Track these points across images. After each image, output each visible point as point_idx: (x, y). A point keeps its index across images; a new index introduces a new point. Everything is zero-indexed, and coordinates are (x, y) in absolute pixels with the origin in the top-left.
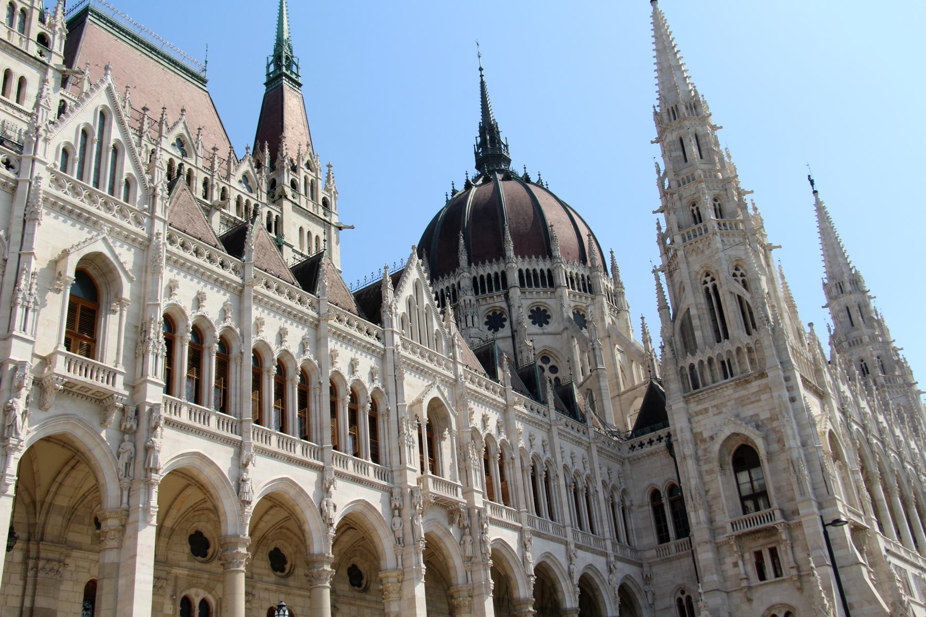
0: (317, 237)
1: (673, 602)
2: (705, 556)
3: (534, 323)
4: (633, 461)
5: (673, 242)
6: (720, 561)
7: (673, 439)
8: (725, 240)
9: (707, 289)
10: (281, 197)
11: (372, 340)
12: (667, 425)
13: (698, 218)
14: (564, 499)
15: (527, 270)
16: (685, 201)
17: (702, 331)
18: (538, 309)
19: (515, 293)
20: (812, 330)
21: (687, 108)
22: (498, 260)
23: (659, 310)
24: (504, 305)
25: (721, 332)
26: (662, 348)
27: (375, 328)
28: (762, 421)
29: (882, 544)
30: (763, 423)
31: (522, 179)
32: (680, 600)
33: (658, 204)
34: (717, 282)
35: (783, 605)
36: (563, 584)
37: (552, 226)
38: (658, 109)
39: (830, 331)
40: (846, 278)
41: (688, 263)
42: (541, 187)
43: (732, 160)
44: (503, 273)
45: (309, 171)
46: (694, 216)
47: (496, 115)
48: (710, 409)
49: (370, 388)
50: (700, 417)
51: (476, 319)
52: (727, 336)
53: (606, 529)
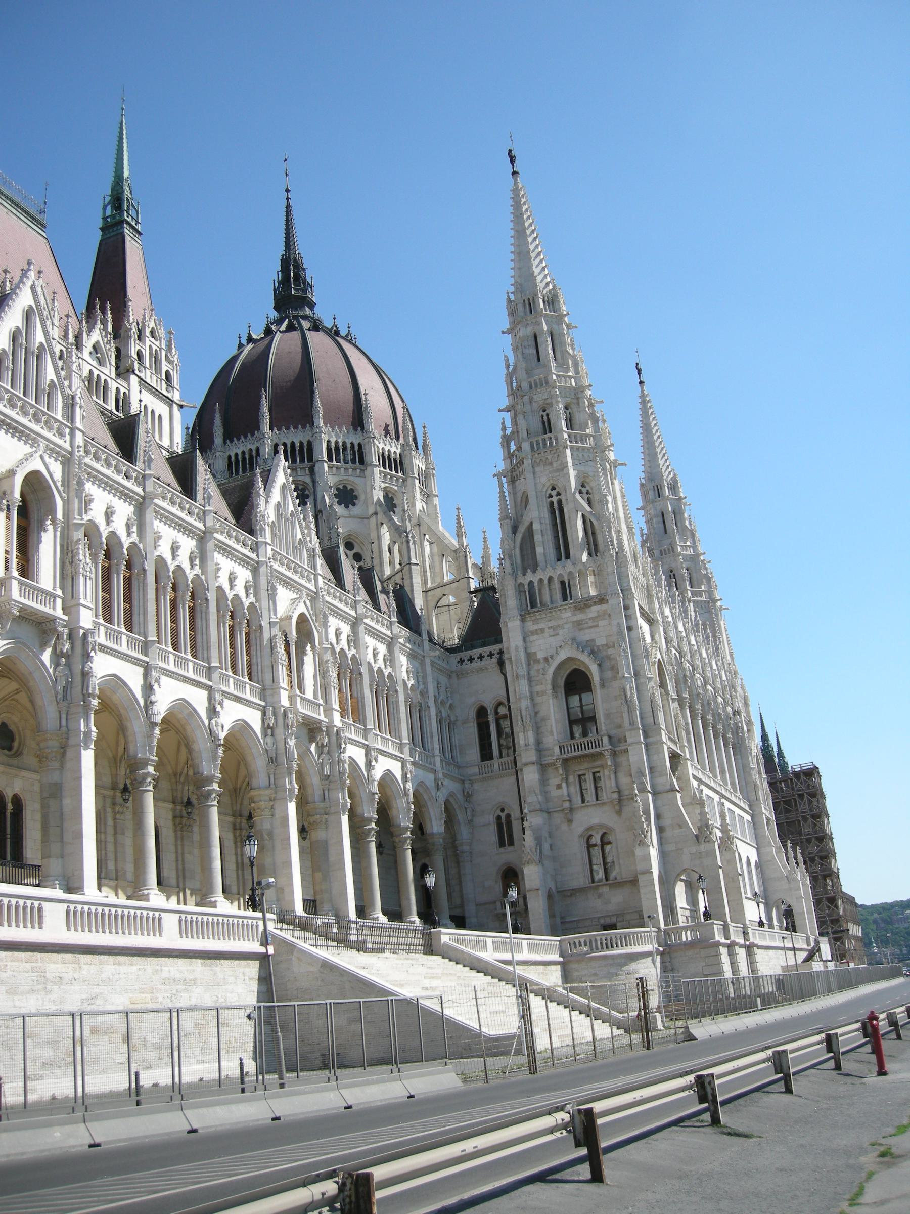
1: (492, 819)
2: (530, 776)
4: (460, 675)
5: (519, 448)
6: (544, 782)
7: (506, 656)
8: (575, 454)
9: (552, 503)
10: (128, 371)
11: (246, 552)
12: (499, 641)
13: (547, 426)
16: (535, 406)
17: (544, 547)
18: (345, 487)
21: (544, 302)
22: (304, 427)
23: (500, 520)
24: (308, 480)
26: (500, 560)
27: (250, 540)
28: (598, 647)
29: (691, 771)
30: (599, 650)
31: (330, 330)
32: (499, 818)
33: (505, 402)
34: (563, 497)
35: (601, 826)
37: (366, 394)
38: (512, 297)
41: (534, 473)
42: (350, 342)
44: (310, 443)
45: (153, 340)
46: (543, 423)
47: (302, 247)
48: (547, 630)
49: (246, 603)
52: (568, 556)
53: (436, 746)
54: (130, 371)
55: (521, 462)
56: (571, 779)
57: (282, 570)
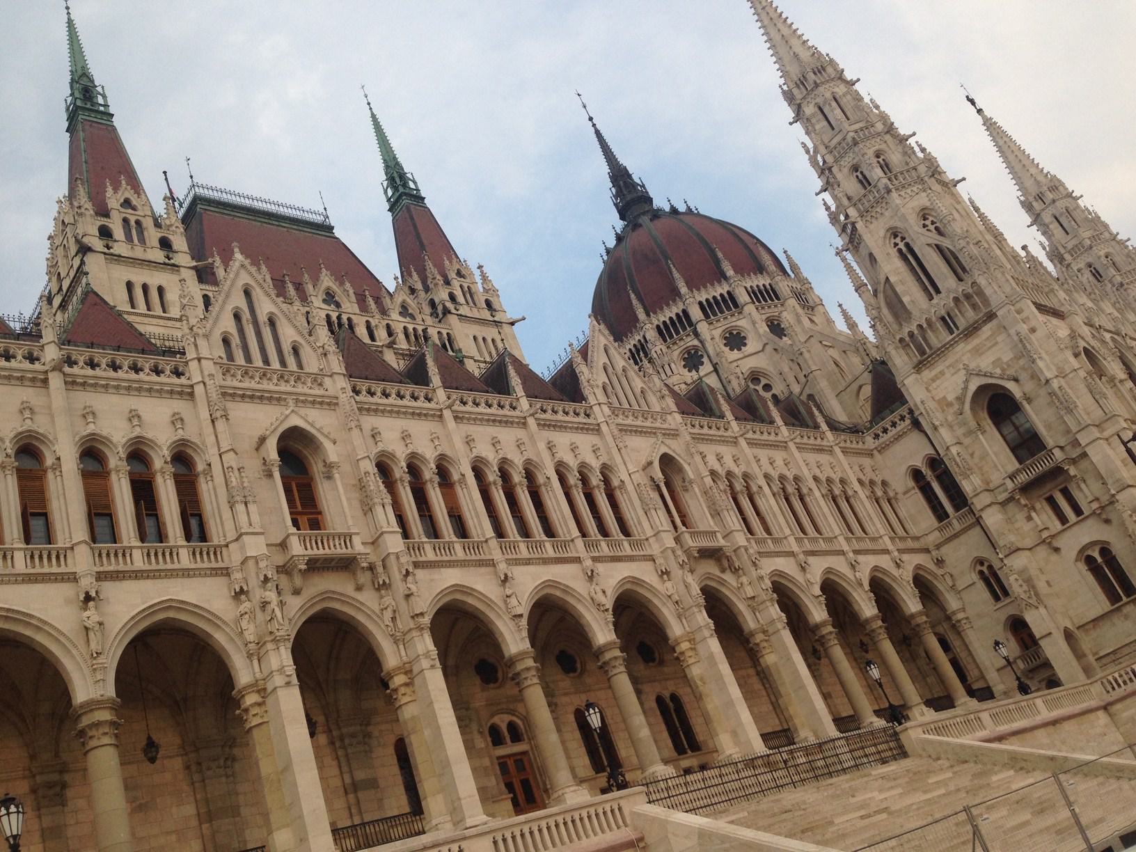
0: (493, 340)
1: (975, 577)
2: (993, 519)
3: (732, 349)
5: (847, 216)
7: (917, 413)
9: (900, 251)
12: (903, 401)
14: (826, 510)
15: (707, 300)
16: (846, 170)
19: (703, 327)
20: (1028, 253)
22: (674, 301)
24: (696, 342)
26: (873, 326)
28: (1007, 363)
30: (1009, 366)
32: (981, 573)
33: (819, 184)
36: (855, 594)
38: (785, 88)
39: (1044, 248)
43: (882, 109)
44: (684, 311)
47: (623, 160)
50: (938, 382)
51: (673, 365)
52: (938, 291)
53: (879, 526)
54: (446, 311)
55: (854, 229)
56: (1038, 506)
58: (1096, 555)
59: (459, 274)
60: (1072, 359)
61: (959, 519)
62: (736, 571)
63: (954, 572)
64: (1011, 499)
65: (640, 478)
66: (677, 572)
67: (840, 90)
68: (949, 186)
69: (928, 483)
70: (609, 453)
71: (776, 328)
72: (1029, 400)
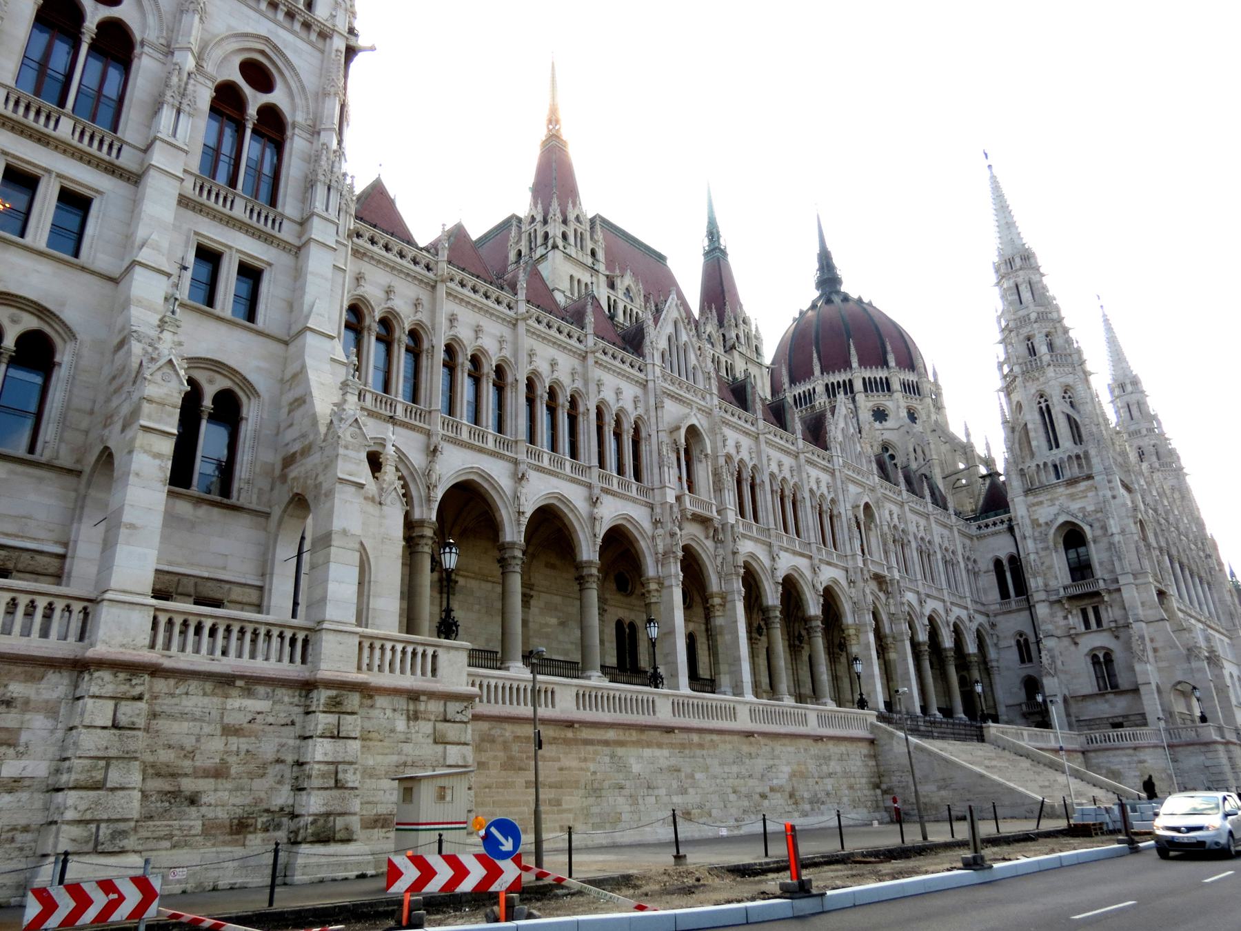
1: (1013, 643)
2: (1042, 610)
4: (980, 537)
5: (1011, 370)
7: (1014, 523)
9: (1041, 408)
13: (1032, 351)
16: (1021, 337)
19: (860, 398)
25: (1053, 442)
29: (1175, 605)
32: (1018, 641)
33: (999, 337)
34: (1049, 403)
40: (1127, 381)
44: (850, 381)
52: (1058, 446)
53: (967, 589)
54: (733, 347)
55: (1014, 380)
56: (1074, 612)
57: (850, 473)
58: (1101, 656)
59: (744, 322)
60: (1132, 525)
61: (1017, 602)
62: (887, 593)
63: (1001, 635)
64: (1059, 601)
65: (850, 513)
66: (860, 584)
67: (1035, 278)
68: (1086, 374)
69: (1004, 572)
70: (835, 491)
71: (912, 417)
72: (1095, 542)
